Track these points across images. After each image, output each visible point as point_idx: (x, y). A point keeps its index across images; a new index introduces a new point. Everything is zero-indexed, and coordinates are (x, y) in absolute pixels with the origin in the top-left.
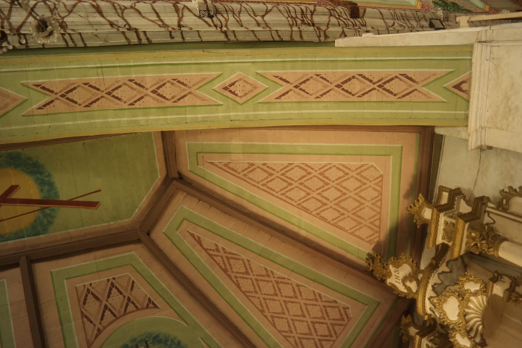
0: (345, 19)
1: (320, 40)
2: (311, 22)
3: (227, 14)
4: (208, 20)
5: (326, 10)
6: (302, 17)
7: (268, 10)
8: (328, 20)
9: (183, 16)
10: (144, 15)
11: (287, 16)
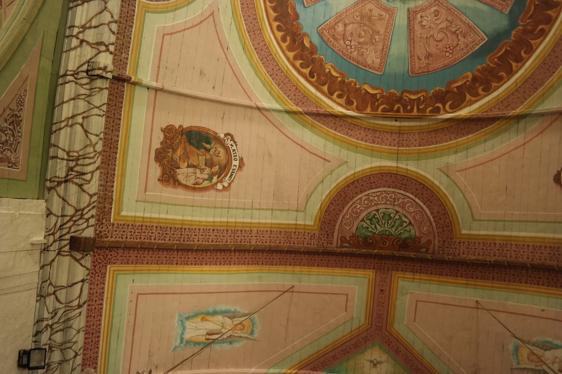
0: (70, 228)
1: (47, 180)
2: (70, 179)
3: (89, 89)
4: (85, 68)
5: (82, 206)
6: (77, 172)
7: (87, 133)
8: (70, 203)
9: (92, 47)
10: (98, 16)
11: (81, 153)
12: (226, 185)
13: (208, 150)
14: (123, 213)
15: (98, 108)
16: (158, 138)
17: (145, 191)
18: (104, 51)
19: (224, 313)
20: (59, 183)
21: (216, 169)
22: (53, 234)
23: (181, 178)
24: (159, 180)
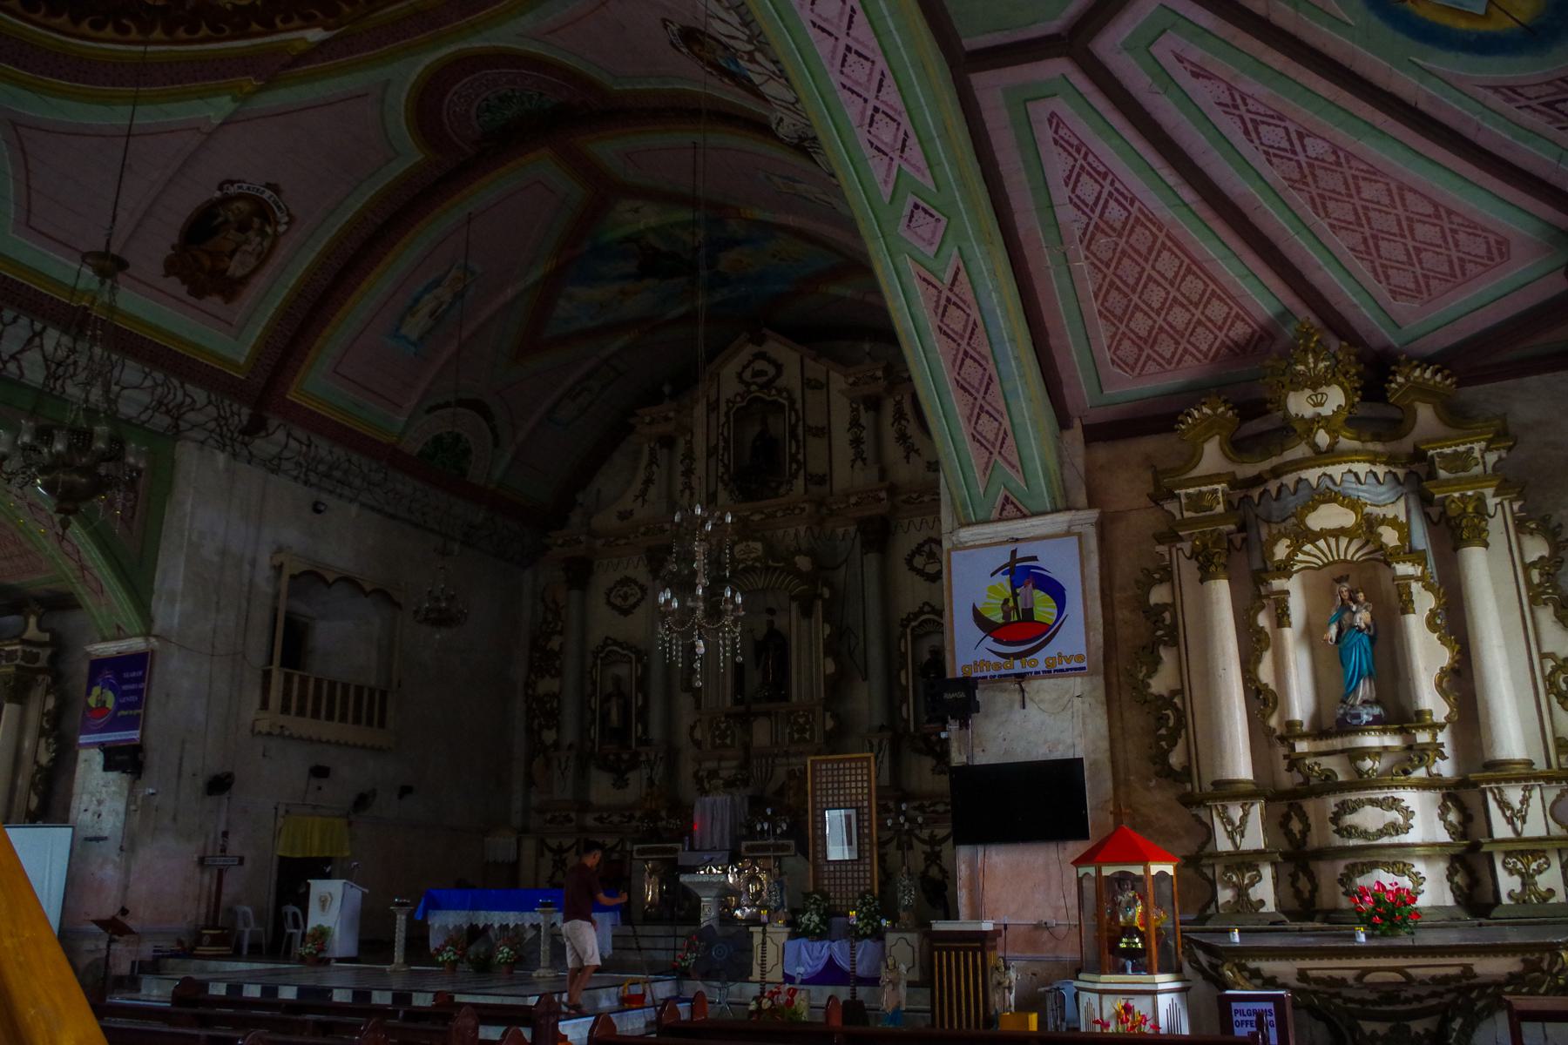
5: (216, 415)
12: (286, 219)
13: (226, 222)
14: (242, 360)
15: (113, 368)
16: (175, 286)
17: (231, 325)
18: (42, 339)
19: (427, 289)
20: (177, 426)
21: (257, 222)
22: (225, 445)
23: (239, 273)
24: (226, 303)
